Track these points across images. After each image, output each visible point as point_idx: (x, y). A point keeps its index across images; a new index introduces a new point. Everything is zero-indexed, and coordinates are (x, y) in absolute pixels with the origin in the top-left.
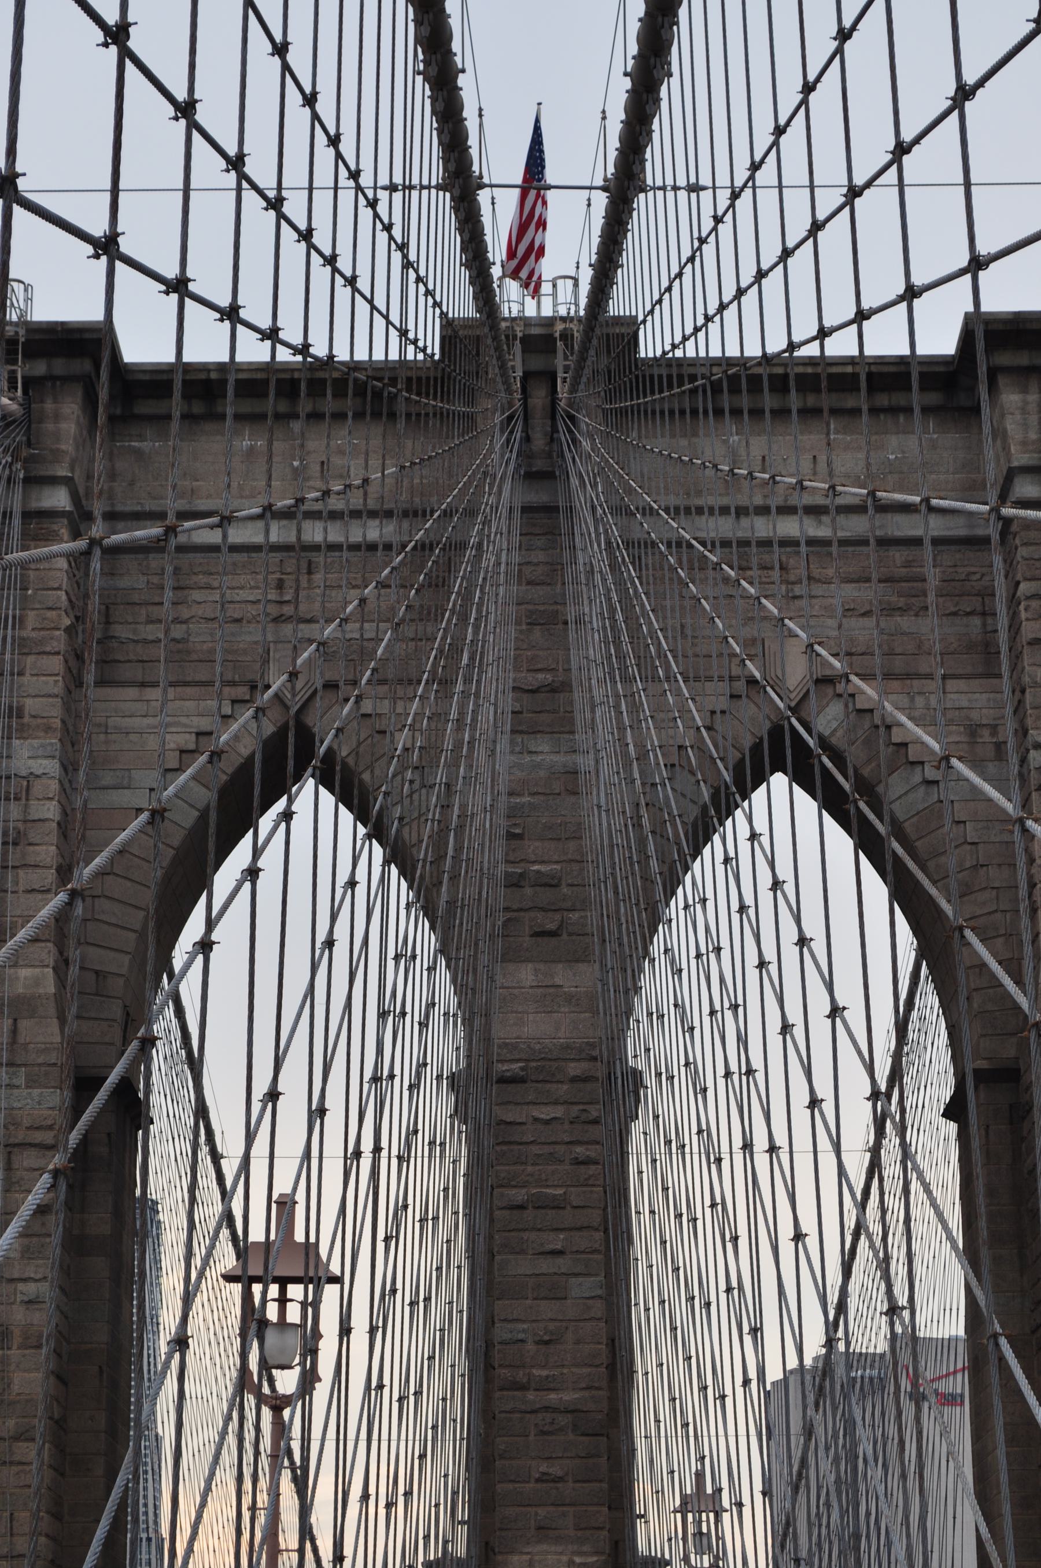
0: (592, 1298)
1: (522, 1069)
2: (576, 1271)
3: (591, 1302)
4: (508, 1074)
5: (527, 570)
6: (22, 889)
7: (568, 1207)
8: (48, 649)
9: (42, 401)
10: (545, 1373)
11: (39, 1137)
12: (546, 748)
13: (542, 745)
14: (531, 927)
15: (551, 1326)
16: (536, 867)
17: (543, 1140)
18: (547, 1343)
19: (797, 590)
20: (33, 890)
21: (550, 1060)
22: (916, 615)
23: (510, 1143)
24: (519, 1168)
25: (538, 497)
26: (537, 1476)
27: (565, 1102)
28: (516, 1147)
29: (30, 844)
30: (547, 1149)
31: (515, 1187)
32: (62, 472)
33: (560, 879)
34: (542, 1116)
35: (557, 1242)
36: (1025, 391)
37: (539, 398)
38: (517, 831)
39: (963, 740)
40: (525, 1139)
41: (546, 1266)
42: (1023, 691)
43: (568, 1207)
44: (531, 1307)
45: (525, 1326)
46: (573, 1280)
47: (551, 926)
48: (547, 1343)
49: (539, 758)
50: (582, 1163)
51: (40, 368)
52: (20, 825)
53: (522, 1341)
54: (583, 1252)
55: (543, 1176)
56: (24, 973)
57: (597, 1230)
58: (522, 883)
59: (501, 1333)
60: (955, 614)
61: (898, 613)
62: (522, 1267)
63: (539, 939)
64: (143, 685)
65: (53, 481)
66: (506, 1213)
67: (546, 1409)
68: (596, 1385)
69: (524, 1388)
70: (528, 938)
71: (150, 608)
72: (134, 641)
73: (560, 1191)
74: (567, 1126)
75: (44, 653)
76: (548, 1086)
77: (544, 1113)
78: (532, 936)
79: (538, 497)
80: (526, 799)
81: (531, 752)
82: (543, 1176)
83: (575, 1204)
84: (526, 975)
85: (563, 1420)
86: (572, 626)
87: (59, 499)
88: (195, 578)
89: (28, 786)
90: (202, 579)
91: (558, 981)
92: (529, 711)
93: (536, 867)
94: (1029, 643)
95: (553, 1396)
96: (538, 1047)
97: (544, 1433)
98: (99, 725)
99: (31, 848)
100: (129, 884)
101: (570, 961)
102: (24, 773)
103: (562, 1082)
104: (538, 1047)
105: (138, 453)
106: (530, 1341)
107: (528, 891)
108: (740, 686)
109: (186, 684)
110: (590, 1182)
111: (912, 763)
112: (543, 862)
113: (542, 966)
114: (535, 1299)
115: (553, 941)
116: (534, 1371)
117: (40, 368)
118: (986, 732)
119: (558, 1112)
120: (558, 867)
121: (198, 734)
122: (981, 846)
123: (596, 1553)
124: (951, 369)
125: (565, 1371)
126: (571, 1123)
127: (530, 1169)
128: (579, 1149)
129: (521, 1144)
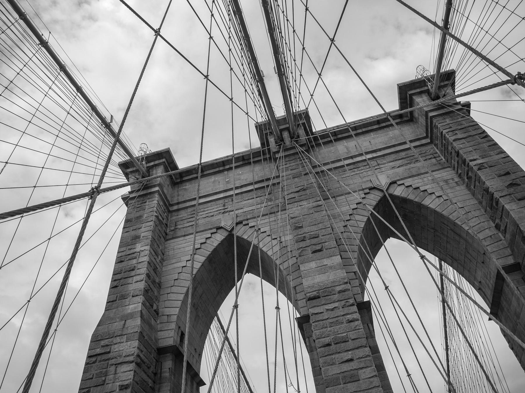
0: (372, 377)
1: (317, 293)
2: (361, 367)
3: (372, 379)
4: (312, 296)
6: (134, 281)
7: (350, 340)
8: (149, 220)
9: (153, 171)
12: (306, 203)
13: (304, 203)
14: (311, 250)
17: (332, 317)
20: (137, 281)
21: (328, 288)
22: (414, 163)
23: (318, 321)
24: (324, 330)
27: (338, 301)
28: (321, 322)
29: (138, 269)
30: (334, 320)
31: (324, 337)
33: (319, 235)
34: (330, 308)
35: (348, 355)
36: (422, 97)
37: (286, 135)
38: (300, 226)
40: (324, 318)
43: (350, 340)
44: (343, 388)
46: (360, 371)
47: (319, 248)
50: (351, 321)
52: (136, 265)
54: (362, 358)
55: (336, 331)
57: (366, 347)
58: (305, 239)
60: (426, 160)
62: (334, 370)
63: (315, 254)
64: (185, 236)
65: (155, 186)
66: (322, 349)
71: (187, 220)
72: (184, 228)
73: (345, 334)
74: (341, 309)
75: (148, 222)
76: (329, 297)
78: (312, 253)
81: (300, 206)
82: (336, 331)
83: (352, 338)
87: (157, 189)
91: (325, 264)
92: (298, 197)
98: (172, 249)
99: (138, 270)
100: (179, 287)
101: (328, 257)
102: (138, 251)
103: (335, 294)
104: (322, 284)
105: (185, 189)
107: (308, 241)
110: (357, 328)
111: (430, 194)
112: (311, 232)
113: (318, 261)
114: (345, 383)
118: (451, 181)
119: (336, 305)
122: (465, 207)
126: (343, 307)
127: (329, 329)
129: (323, 320)
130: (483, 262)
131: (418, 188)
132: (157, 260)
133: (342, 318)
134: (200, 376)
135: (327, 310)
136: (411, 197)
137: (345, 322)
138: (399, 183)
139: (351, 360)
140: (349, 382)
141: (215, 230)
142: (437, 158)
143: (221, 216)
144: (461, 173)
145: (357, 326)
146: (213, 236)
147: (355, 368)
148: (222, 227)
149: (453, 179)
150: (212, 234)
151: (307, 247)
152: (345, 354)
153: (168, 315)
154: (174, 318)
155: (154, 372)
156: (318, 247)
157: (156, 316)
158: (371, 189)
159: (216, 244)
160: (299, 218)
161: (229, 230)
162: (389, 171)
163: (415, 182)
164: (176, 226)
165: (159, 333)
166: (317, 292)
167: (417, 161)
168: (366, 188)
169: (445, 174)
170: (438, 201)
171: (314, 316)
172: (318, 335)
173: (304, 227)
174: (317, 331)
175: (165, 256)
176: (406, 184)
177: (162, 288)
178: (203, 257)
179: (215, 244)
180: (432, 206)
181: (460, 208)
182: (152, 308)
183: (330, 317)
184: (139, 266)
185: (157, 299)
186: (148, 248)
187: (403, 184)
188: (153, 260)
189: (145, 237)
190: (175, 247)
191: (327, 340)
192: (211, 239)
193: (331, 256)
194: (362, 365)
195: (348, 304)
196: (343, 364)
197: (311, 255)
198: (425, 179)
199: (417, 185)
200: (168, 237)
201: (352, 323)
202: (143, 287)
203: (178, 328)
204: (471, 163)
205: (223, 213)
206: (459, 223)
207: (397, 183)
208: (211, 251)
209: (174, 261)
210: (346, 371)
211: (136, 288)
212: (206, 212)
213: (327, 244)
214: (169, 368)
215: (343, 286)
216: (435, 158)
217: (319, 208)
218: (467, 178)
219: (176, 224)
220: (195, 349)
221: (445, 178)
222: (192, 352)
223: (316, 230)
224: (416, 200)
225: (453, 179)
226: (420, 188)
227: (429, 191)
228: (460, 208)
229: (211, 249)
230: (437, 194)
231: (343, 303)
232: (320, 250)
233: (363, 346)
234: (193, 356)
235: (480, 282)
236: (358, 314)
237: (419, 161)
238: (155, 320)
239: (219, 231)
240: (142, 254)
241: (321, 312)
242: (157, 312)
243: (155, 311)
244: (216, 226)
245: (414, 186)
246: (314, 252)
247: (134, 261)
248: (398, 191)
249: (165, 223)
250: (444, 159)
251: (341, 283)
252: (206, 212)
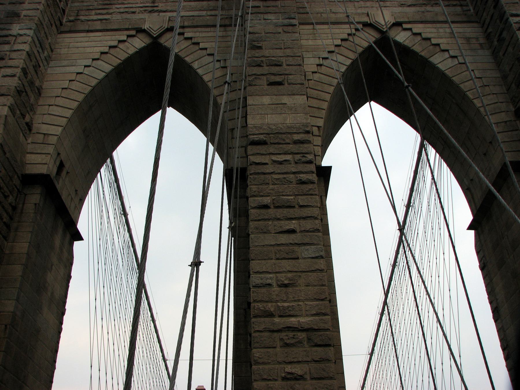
0: (316, 258)
4: (257, 139)
7: (297, 206)
10: (286, 304)
12: (273, 18)
14: (268, 81)
15: (290, 275)
18: (286, 286)
24: (265, 187)
26: (283, 375)
29: (10, 59)
38: (259, 45)
39: (464, 42)
40: (268, 171)
41: (284, 239)
45: (271, 275)
48: (286, 286)
53: (270, 285)
58: (262, 65)
61: (423, 6)
64: (88, 31)
67: (289, 328)
68: (323, 312)
69: (271, 315)
70: (266, 86)
76: (281, 146)
78: (268, 85)
81: (265, 19)
83: (301, 204)
85: (302, 336)
89: (15, 39)
91: (283, 102)
92: (264, 6)
95: (293, 319)
96: (274, 127)
97: (287, 345)
100: (67, 100)
101: (290, 95)
106: (275, 284)
108: (360, 26)
110: (310, 193)
112: (273, 57)
114: (278, 259)
115: (280, 87)
116: (279, 304)
118: (474, 41)
119: (288, 157)
122: (483, 79)
125: (300, 303)
127: (271, 187)
130: (485, 154)
131: (429, 39)
132: (41, 55)
133: (292, 176)
134: (78, 227)
135: (274, 161)
136: (417, 48)
137: (294, 182)
138: (405, 26)
139: (292, 231)
140: (284, 259)
141: (133, 33)
142: (464, 7)
143: (146, 16)
144: (491, 32)
145: (310, 189)
146: (130, 40)
147: (296, 242)
148: (145, 29)
149: (477, 39)
150: (129, 36)
151: (262, 75)
152: (287, 222)
153: (44, 134)
154: (53, 140)
155: (14, 204)
156: (278, 79)
157: (28, 132)
158: (366, 25)
159: (131, 51)
160: (259, 35)
161: (155, 36)
162: (395, 8)
163: (427, 30)
164: (78, 15)
165: (28, 155)
166: (265, 135)
167: (437, 4)
168: (358, 23)
169: (469, 30)
170: (450, 63)
171: (253, 166)
172: (255, 192)
173: (264, 48)
174: (255, 186)
175: (54, 53)
176: (415, 31)
177: (42, 95)
178: (110, 66)
179: (131, 51)
180: (441, 67)
181: (477, 78)
182: (24, 118)
183: (276, 172)
184: (14, 55)
185: (32, 109)
186: (31, 33)
187: (410, 29)
188: (36, 52)
189: (27, 17)
190: (71, 45)
191: (267, 200)
192: (126, 44)
193: (294, 95)
194: (307, 240)
195: (304, 159)
196: (281, 235)
197: (266, 87)
198: (441, 30)
199: (429, 36)
200: (63, 29)
201: (304, 186)
203: (57, 154)
204: (511, 19)
205: (150, 12)
206: (471, 97)
207: (402, 26)
208: (123, 59)
209: (65, 63)
210: (282, 244)
211: (4, 84)
212: (126, 6)
213: (290, 77)
214: (36, 204)
215: (303, 135)
216: (461, 5)
217: (291, 28)
218: (498, 41)
219: (78, 13)
220: (76, 191)
221: (468, 35)
222: (71, 194)
223: (281, 55)
224: (423, 54)
225: (477, 39)
226: (432, 40)
227: (443, 47)
228: (477, 78)
229: (124, 56)
230: (452, 53)
231: (298, 157)
232: (280, 84)
233: (313, 217)
234: (72, 198)
235: (472, 180)
236: (315, 175)
237: (438, 5)
238: (25, 137)
239: (140, 35)
240: (20, 39)
241: (265, 162)
242: (29, 126)
243: (27, 124)
244: (136, 27)
245: (424, 36)
246: (272, 84)
247: (7, 47)
249: (62, 8)
250: (472, 11)
251: (301, 131)
252: (126, 6)
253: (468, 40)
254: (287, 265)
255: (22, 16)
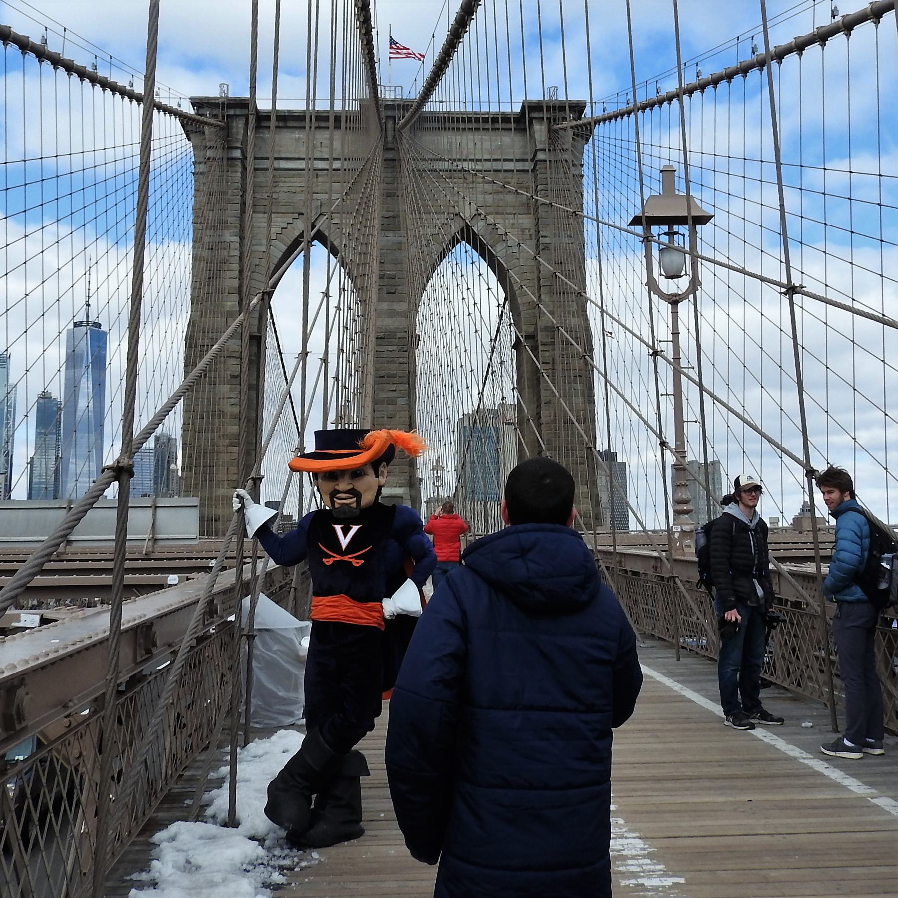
5: (386, 179)
11: (234, 354)
13: (390, 234)
16: (388, 273)
18: (391, 417)
19: (471, 186)
25: (390, 155)
30: (391, 359)
32: (240, 145)
36: (541, 125)
38: (382, 261)
42: (538, 219)
47: (393, 291)
48: (391, 417)
49: (389, 238)
51: (232, 112)
53: (383, 417)
56: (229, 303)
59: (377, 414)
62: (383, 395)
65: (237, 148)
77: (390, 348)
79: (390, 155)
80: (385, 251)
84: (385, 306)
86: (400, 197)
88: (280, 179)
90: (283, 179)
93: (388, 273)
94: (541, 205)
109: (278, 213)
113: (389, 303)
117: (232, 112)
120: (394, 273)
121: (282, 229)
123: (405, 480)
124: (519, 116)
128: (400, 359)
194: (401, 395)
202: (238, 286)
208: (292, 240)
232: (393, 293)
247: (225, 253)
248: (478, 227)
253: (523, 230)
254: (391, 407)
255: (229, 224)
